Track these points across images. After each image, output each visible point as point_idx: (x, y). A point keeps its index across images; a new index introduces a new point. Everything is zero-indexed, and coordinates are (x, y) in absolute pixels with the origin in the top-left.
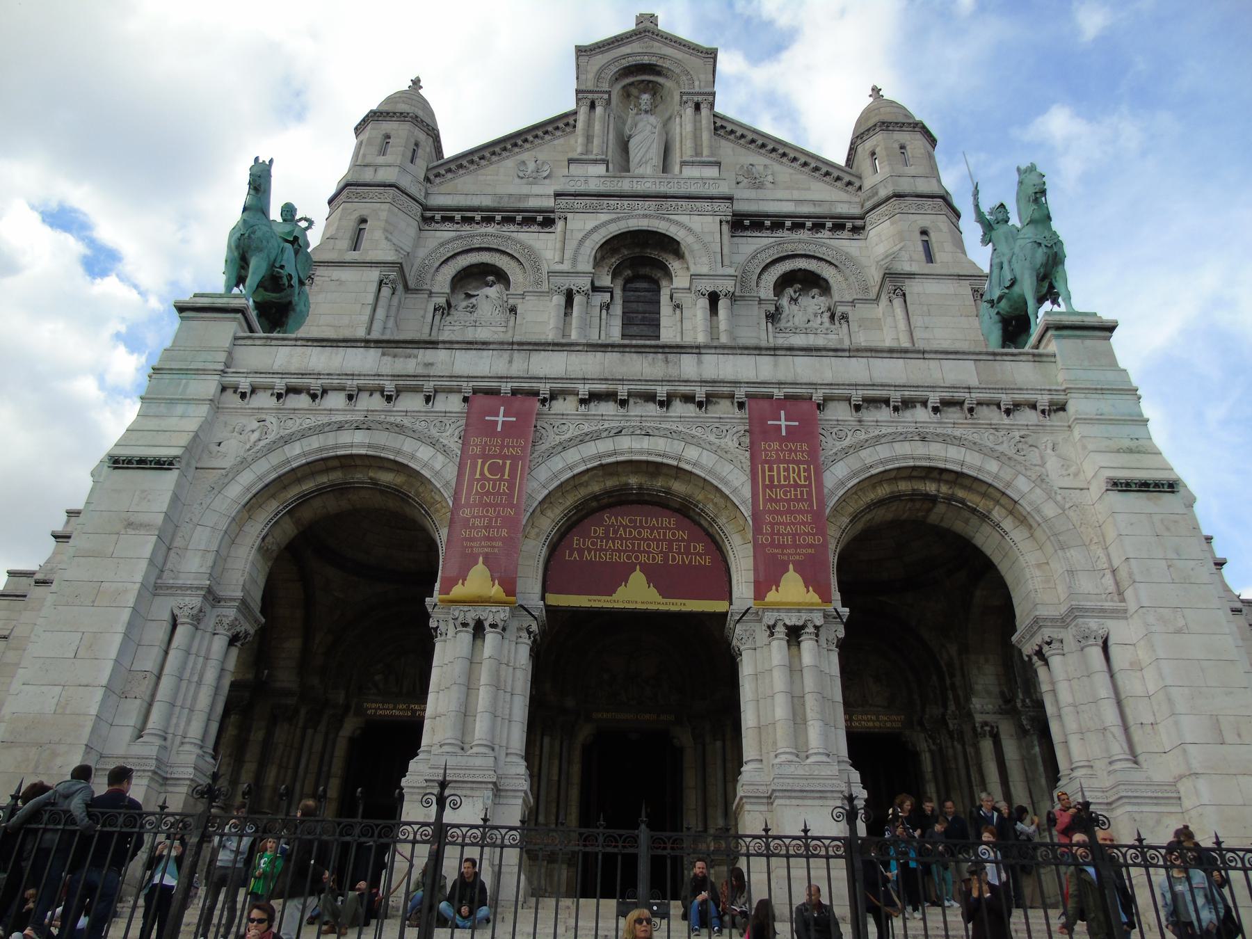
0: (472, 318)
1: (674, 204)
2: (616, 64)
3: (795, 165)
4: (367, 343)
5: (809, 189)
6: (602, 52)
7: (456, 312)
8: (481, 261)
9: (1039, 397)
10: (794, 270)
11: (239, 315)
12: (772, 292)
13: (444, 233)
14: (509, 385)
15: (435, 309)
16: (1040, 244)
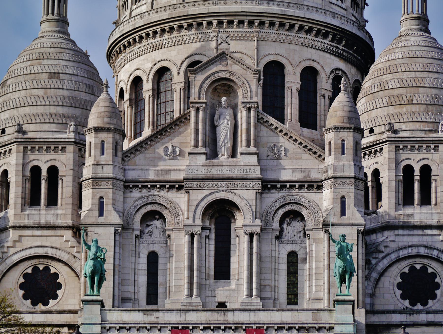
0: (152, 239)
1: (236, 183)
2: (209, 79)
3: (296, 143)
4: (139, 311)
5: (300, 159)
6: (202, 71)
7: (143, 236)
8: (152, 209)
9: (326, 326)
10: (289, 210)
11: (100, 303)
12: (278, 224)
13: (136, 194)
14: (181, 326)
15: (136, 237)
16: (340, 267)
